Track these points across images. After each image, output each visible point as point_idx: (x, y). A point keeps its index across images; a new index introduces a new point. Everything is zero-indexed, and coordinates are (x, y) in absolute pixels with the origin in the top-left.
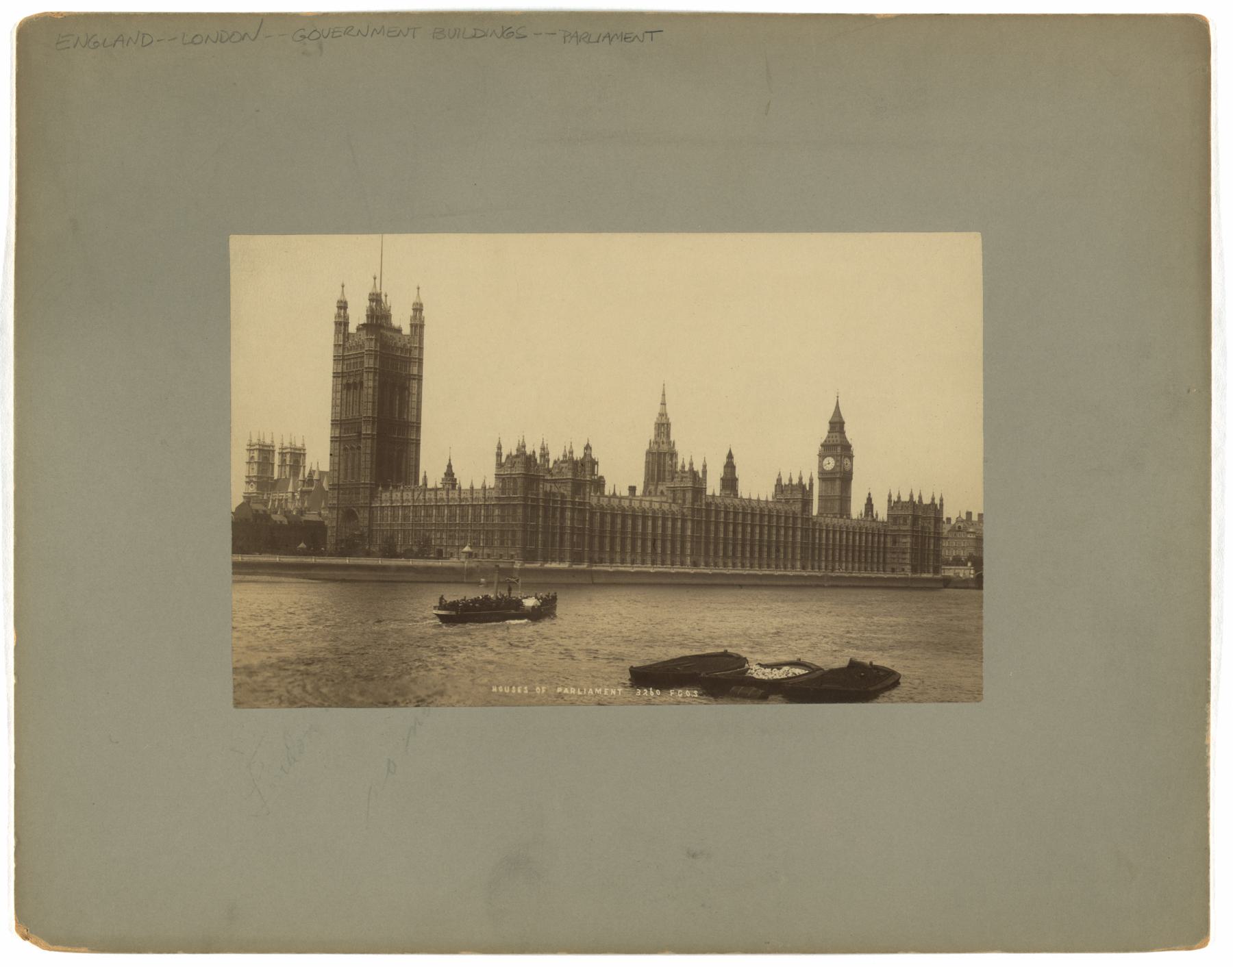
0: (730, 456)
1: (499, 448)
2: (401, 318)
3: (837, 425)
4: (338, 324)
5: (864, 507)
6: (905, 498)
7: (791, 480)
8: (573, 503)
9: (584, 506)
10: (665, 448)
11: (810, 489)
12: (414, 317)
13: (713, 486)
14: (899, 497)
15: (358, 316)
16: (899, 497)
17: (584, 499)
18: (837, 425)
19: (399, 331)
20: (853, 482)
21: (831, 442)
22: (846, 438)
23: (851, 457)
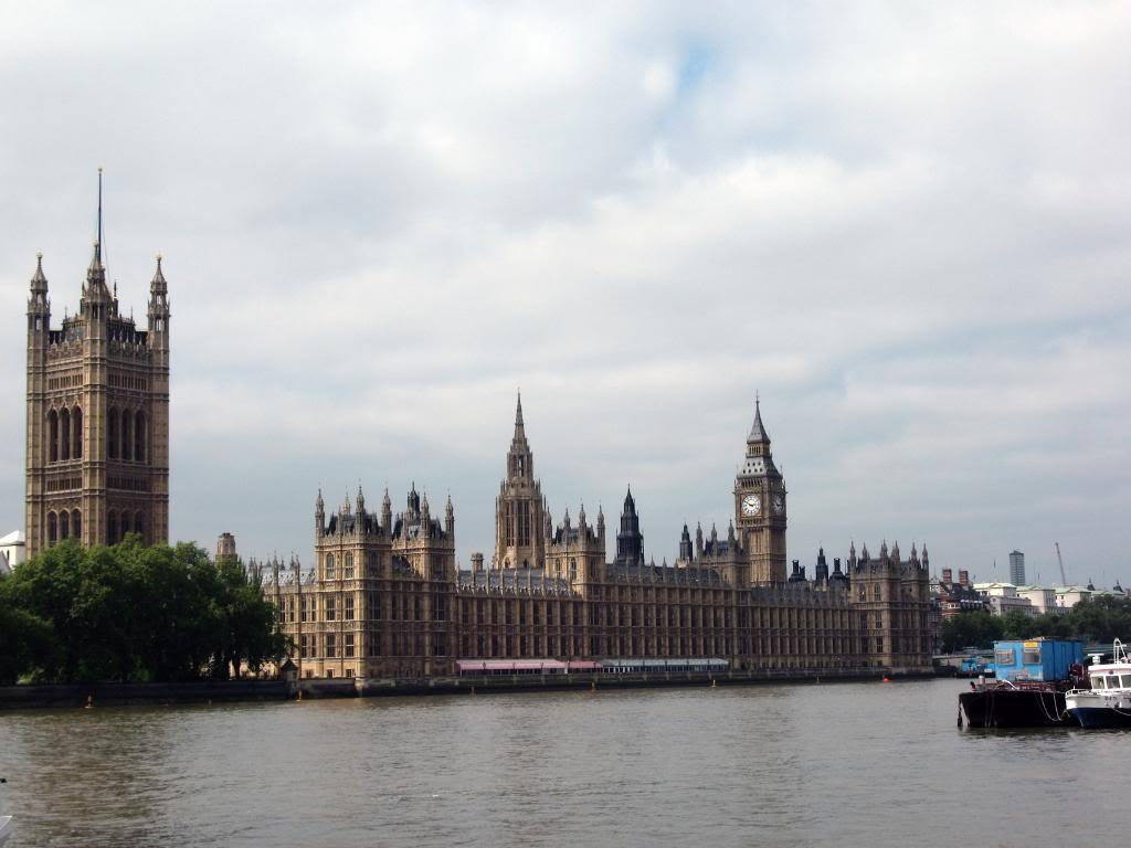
0: (630, 503)
1: (321, 505)
2: (134, 307)
3: (761, 446)
4: (33, 318)
5: (815, 572)
6: (875, 555)
7: (714, 534)
8: (431, 584)
9: (448, 589)
10: (526, 492)
11: (744, 546)
12: (153, 304)
13: (611, 552)
14: (865, 553)
15: (65, 304)
16: (865, 553)
17: (445, 578)
18: (761, 446)
19: (128, 327)
20: (788, 532)
21: (753, 471)
22: (772, 465)
23: (783, 494)
